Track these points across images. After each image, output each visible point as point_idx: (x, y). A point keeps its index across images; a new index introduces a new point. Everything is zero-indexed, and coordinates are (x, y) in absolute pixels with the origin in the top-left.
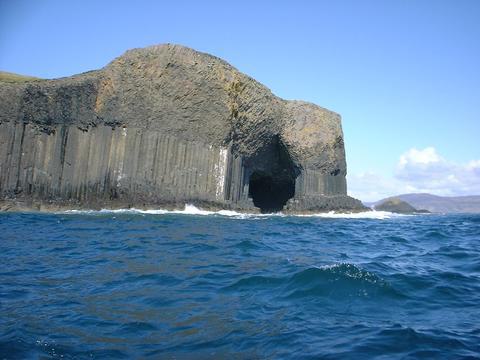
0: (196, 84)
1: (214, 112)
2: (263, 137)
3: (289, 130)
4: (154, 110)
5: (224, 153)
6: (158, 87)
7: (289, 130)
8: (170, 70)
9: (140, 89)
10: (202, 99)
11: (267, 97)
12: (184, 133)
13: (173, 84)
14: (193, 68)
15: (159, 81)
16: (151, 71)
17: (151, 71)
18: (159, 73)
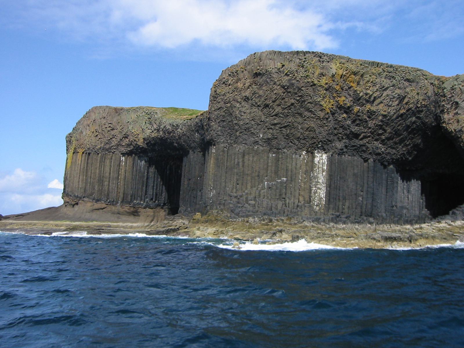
0: (283, 87)
1: (307, 114)
2: (411, 130)
3: (451, 115)
4: (241, 123)
5: (321, 158)
6: (246, 99)
7: (451, 115)
8: (259, 80)
9: (229, 105)
10: (293, 101)
11: (408, 80)
12: (274, 142)
13: (261, 92)
14: (279, 71)
15: (247, 93)
16: (240, 85)
17: (240, 85)
18: (247, 85)
